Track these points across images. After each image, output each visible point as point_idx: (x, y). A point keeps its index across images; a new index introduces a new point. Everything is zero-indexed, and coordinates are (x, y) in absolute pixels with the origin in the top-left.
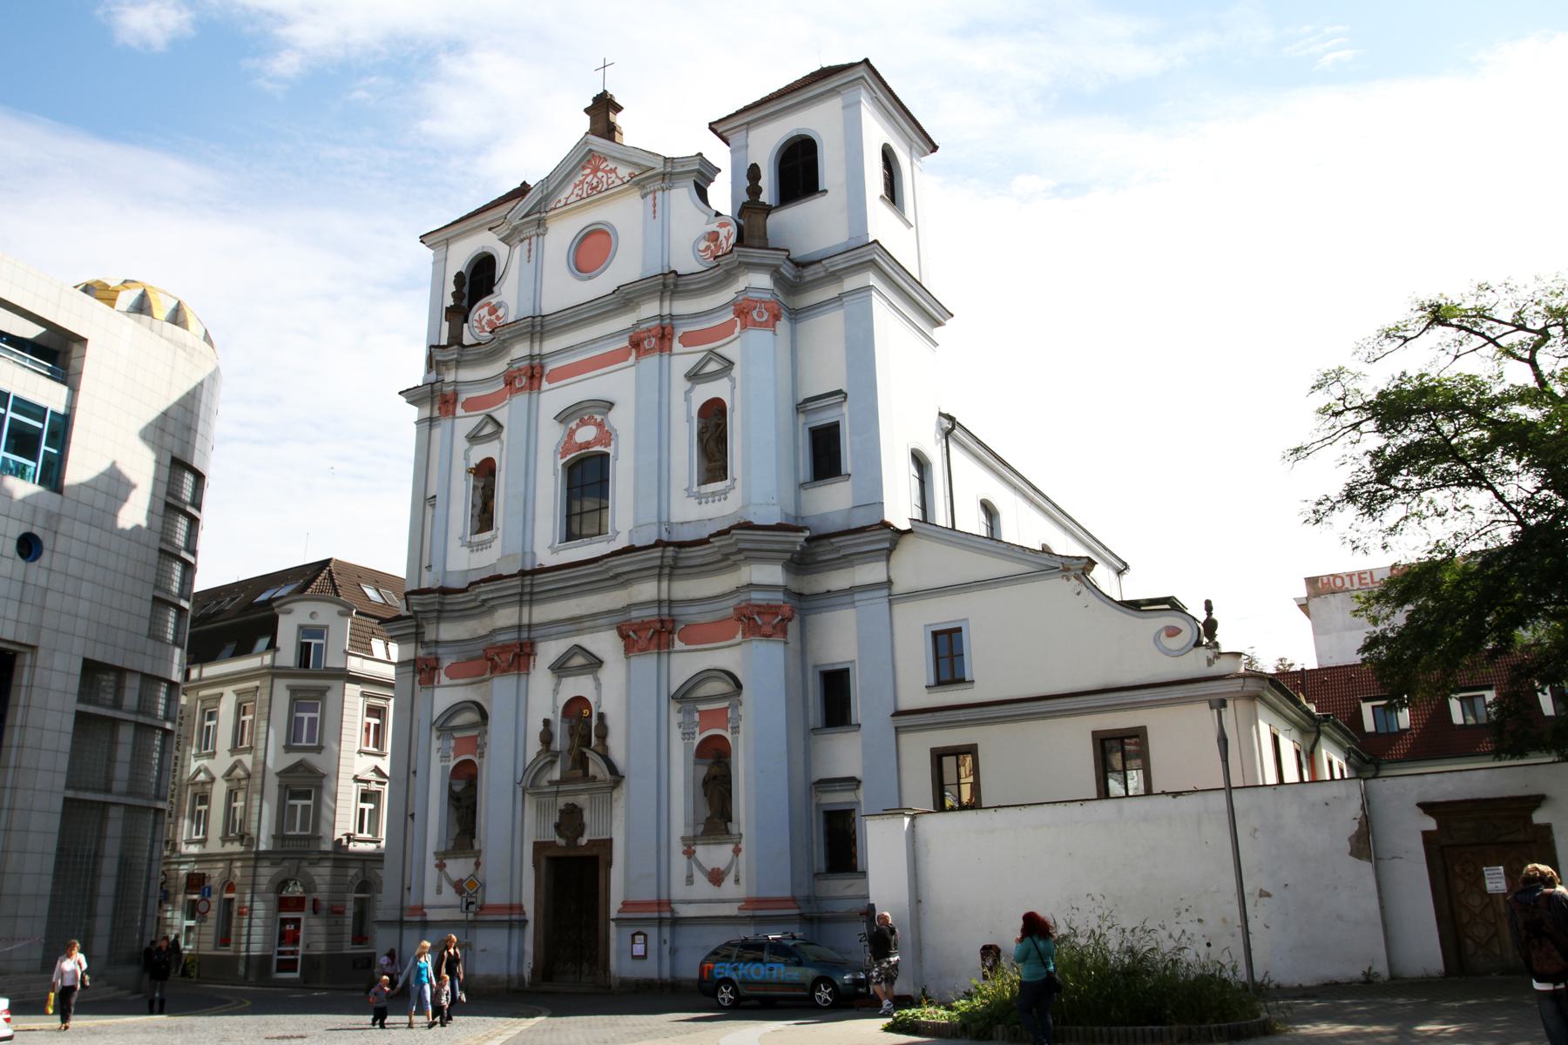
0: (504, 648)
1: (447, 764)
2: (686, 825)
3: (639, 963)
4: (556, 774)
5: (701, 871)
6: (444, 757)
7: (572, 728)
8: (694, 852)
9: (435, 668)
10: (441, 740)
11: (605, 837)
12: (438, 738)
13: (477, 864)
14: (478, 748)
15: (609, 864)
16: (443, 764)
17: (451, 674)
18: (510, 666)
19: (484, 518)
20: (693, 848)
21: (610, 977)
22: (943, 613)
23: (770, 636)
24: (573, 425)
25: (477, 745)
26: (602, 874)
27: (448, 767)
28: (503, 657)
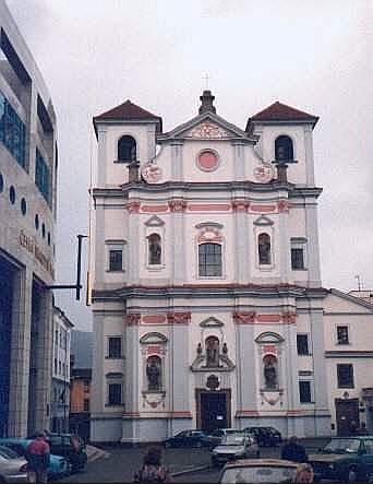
19: (155, 255)
22: (342, 321)
24: (204, 229)
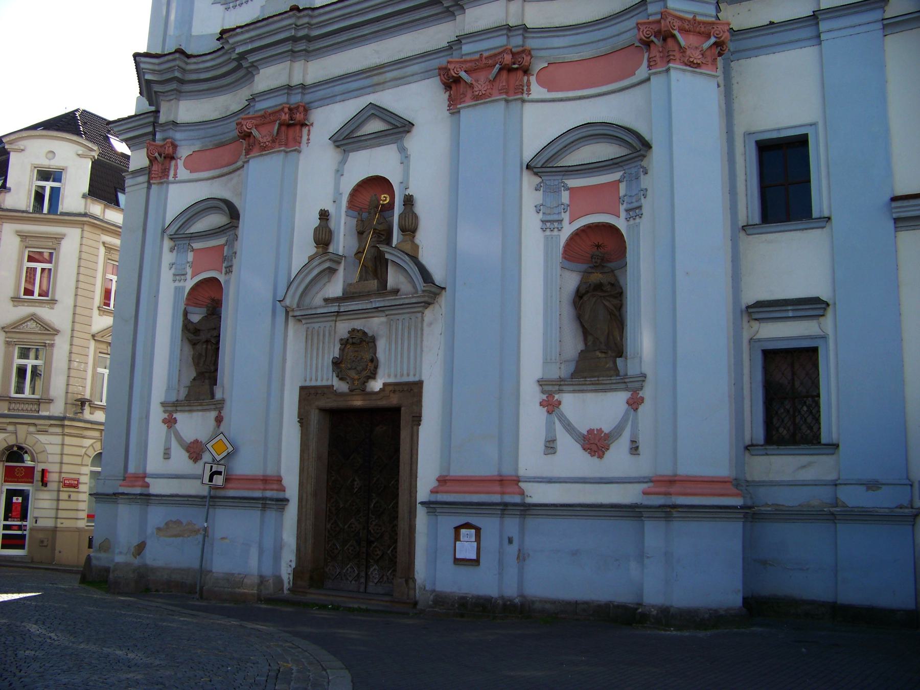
0: (265, 118)
1: (181, 284)
2: (546, 362)
3: (464, 570)
4: (335, 288)
5: (571, 434)
6: (179, 275)
7: (361, 221)
8: (560, 403)
9: (171, 157)
10: (175, 252)
11: (411, 379)
12: (172, 250)
13: (219, 420)
14: (223, 262)
15: (417, 419)
16: (177, 284)
17: (191, 166)
18: (273, 141)
20: (557, 397)
21: (415, 589)
23: (698, 65)
25: (227, 261)
26: (404, 435)
27: (184, 288)
28: (265, 130)
